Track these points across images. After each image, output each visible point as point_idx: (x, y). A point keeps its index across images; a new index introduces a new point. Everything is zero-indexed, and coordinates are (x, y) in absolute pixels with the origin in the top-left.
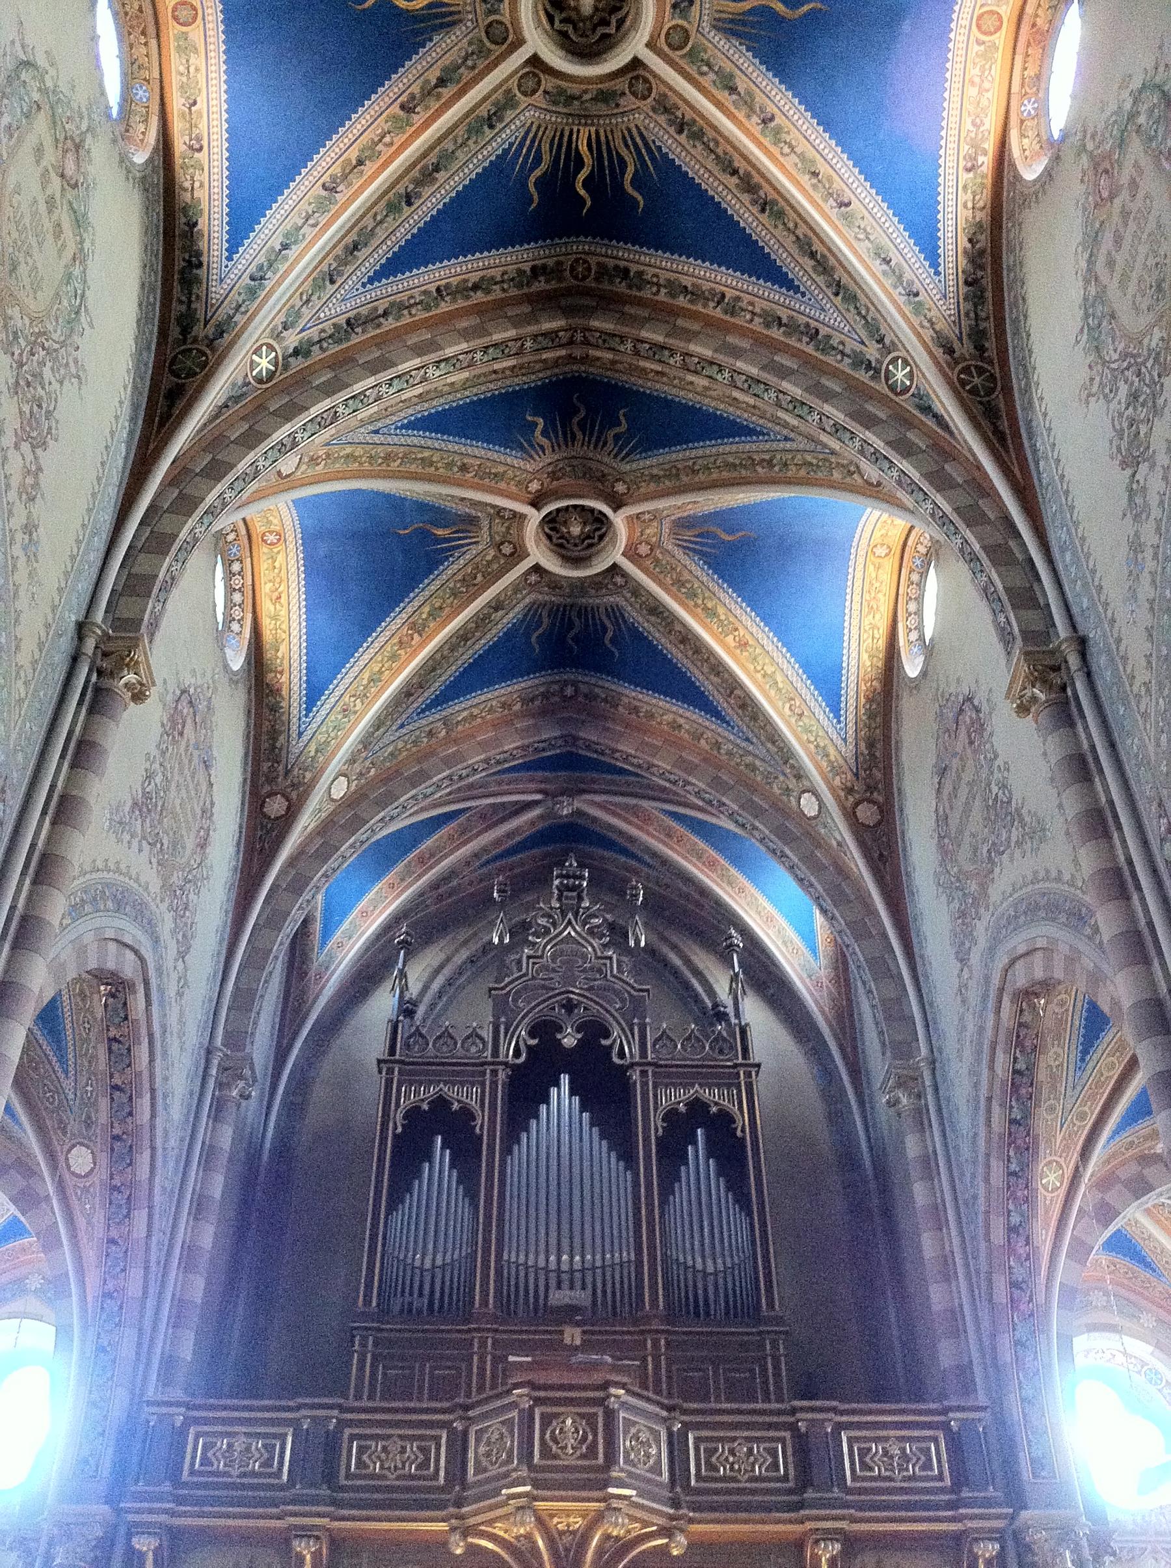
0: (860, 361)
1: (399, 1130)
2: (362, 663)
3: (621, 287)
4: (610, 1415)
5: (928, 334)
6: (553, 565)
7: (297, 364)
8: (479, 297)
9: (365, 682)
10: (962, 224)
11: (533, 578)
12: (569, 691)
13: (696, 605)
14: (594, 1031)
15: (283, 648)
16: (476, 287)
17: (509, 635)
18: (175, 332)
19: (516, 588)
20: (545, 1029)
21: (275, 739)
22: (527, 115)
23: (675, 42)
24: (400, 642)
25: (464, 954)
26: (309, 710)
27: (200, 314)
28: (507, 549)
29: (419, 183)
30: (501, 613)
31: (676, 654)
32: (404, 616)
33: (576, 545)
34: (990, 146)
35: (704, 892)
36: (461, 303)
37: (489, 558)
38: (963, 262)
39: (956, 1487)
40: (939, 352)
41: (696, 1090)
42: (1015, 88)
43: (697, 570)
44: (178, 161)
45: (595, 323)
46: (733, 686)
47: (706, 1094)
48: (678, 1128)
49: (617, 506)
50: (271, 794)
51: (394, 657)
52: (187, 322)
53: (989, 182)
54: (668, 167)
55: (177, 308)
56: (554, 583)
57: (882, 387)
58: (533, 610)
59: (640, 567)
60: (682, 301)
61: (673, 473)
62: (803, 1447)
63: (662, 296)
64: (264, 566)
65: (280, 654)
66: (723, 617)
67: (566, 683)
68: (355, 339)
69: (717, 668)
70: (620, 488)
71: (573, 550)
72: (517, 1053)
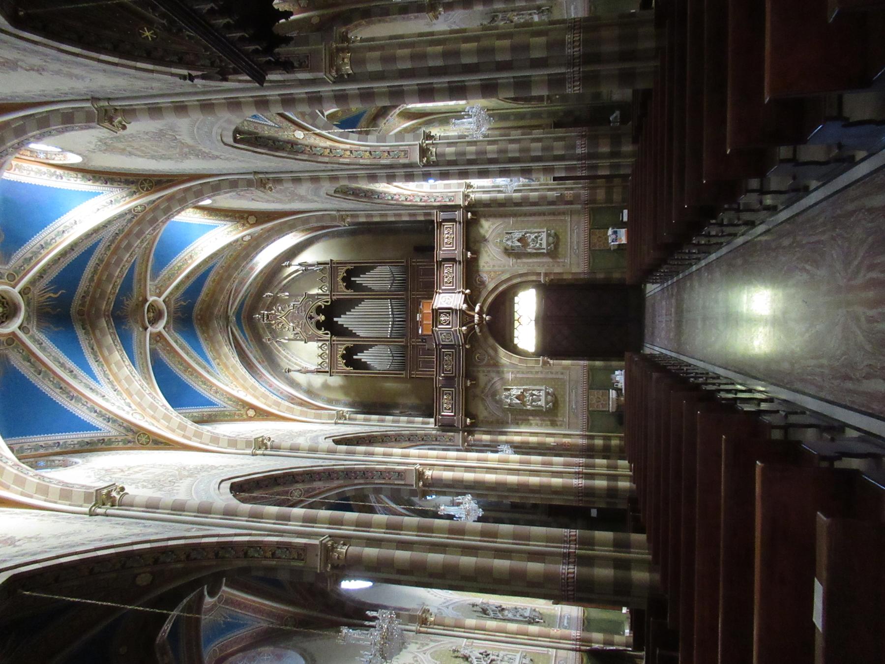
0: (130, 221)
3: (88, 299)
5: (128, 199)
7: (134, 407)
8: (95, 347)
10: (83, 182)
14: (319, 310)
16: (93, 349)
18: (130, 445)
20: (319, 325)
22: (34, 331)
23: (13, 278)
29: (65, 368)
34: (53, 170)
35: (261, 272)
36: (99, 354)
38: (98, 184)
39: (456, 222)
40: (135, 197)
41: (339, 279)
42: (33, 159)
43: (165, 272)
44: (63, 450)
45: (104, 307)
46: (205, 262)
47: (340, 277)
48: (350, 285)
53: (66, 172)
54: (52, 283)
56: (167, 323)
57: (141, 214)
60: (96, 278)
61: (139, 281)
63: (93, 284)
68: (119, 389)
69: (199, 266)
70: (141, 299)
71: (157, 316)
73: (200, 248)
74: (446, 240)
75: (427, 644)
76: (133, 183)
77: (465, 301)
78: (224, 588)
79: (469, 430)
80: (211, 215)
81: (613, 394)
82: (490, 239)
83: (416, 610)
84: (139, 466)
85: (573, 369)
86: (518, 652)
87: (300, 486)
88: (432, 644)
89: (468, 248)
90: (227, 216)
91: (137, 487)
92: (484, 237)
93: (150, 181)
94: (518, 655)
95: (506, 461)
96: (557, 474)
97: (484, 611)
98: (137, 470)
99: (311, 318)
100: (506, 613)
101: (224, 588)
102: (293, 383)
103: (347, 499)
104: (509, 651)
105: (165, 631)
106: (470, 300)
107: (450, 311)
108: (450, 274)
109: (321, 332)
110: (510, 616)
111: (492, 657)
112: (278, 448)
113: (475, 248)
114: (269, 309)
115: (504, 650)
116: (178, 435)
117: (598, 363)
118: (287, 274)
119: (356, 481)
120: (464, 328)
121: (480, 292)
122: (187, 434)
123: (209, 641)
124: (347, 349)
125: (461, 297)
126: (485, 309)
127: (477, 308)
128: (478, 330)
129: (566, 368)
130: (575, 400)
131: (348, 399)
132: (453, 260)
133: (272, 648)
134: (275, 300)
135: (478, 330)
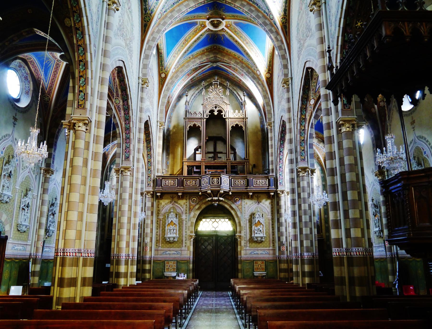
0: (265, 12)
4: (221, 178)
6: (211, 28)
7: (165, 14)
12: (215, 47)
14: (220, 112)
15: (162, 45)
17: (203, 40)
18: (144, 12)
19: (205, 32)
20: (212, 111)
25: (197, 92)
26: (167, 56)
27: (148, 8)
28: (203, 26)
31: (235, 43)
39: (268, 186)
46: (245, 51)
50: (162, 73)
51: (182, 46)
52: (146, 10)
55: (144, 7)
56: (212, 31)
57: (268, 17)
58: (208, 35)
59: (228, 29)
61: (234, 16)
62: (248, 181)
67: (214, 46)
68: (174, 6)
69: (242, 47)
72: (207, 116)
73: (252, 48)
74: (258, 181)
75: (34, 174)
76: (285, 13)
77: (225, 192)
78: (65, 63)
79: (154, 195)
80: (270, 54)
81: (174, 274)
82: (259, 205)
83: (53, 167)
84: (132, 17)
85: (187, 252)
86: (30, 224)
87: (121, 103)
88: (34, 176)
89: (254, 193)
90: (270, 62)
91: (119, 17)
92: (261, 202)
93: (286, 23)
94: (28, 224)
95: (135, 216)
96: (126, 245)
97: (53, 205)
98: (130, 16)
99: (216, 107)
100: (52, 217)
101: (65, 63)
102: (180, 97)
103: (114, 128)
104: (30, 219)
105: (40, 33)
106: (226, 195)
107: (220, 183)
108: (240, 182)
109: (208, 111)
110: (50, 219)
111: (26, 209)
112: (142, 91)
113: (254, 197)
114: (221, 84)
115: (31, 216)
116: (149, 37)
117: (191, 266)
118: (240, 94)
119: (124, 134)
120: (210, 191)
121: (230, 200)
122: (150, 42)
123: (36, 56)
124: (199, 127)
125: (227, 189)
126: (221, 203)
127: (221, 199)
128: (209, 199)
129: (188, 249)
130: (171, 253)
131: (171, 128)
132: (248, 185)
133: (32, 89)
134: (225, 87)
135: (209, 199)
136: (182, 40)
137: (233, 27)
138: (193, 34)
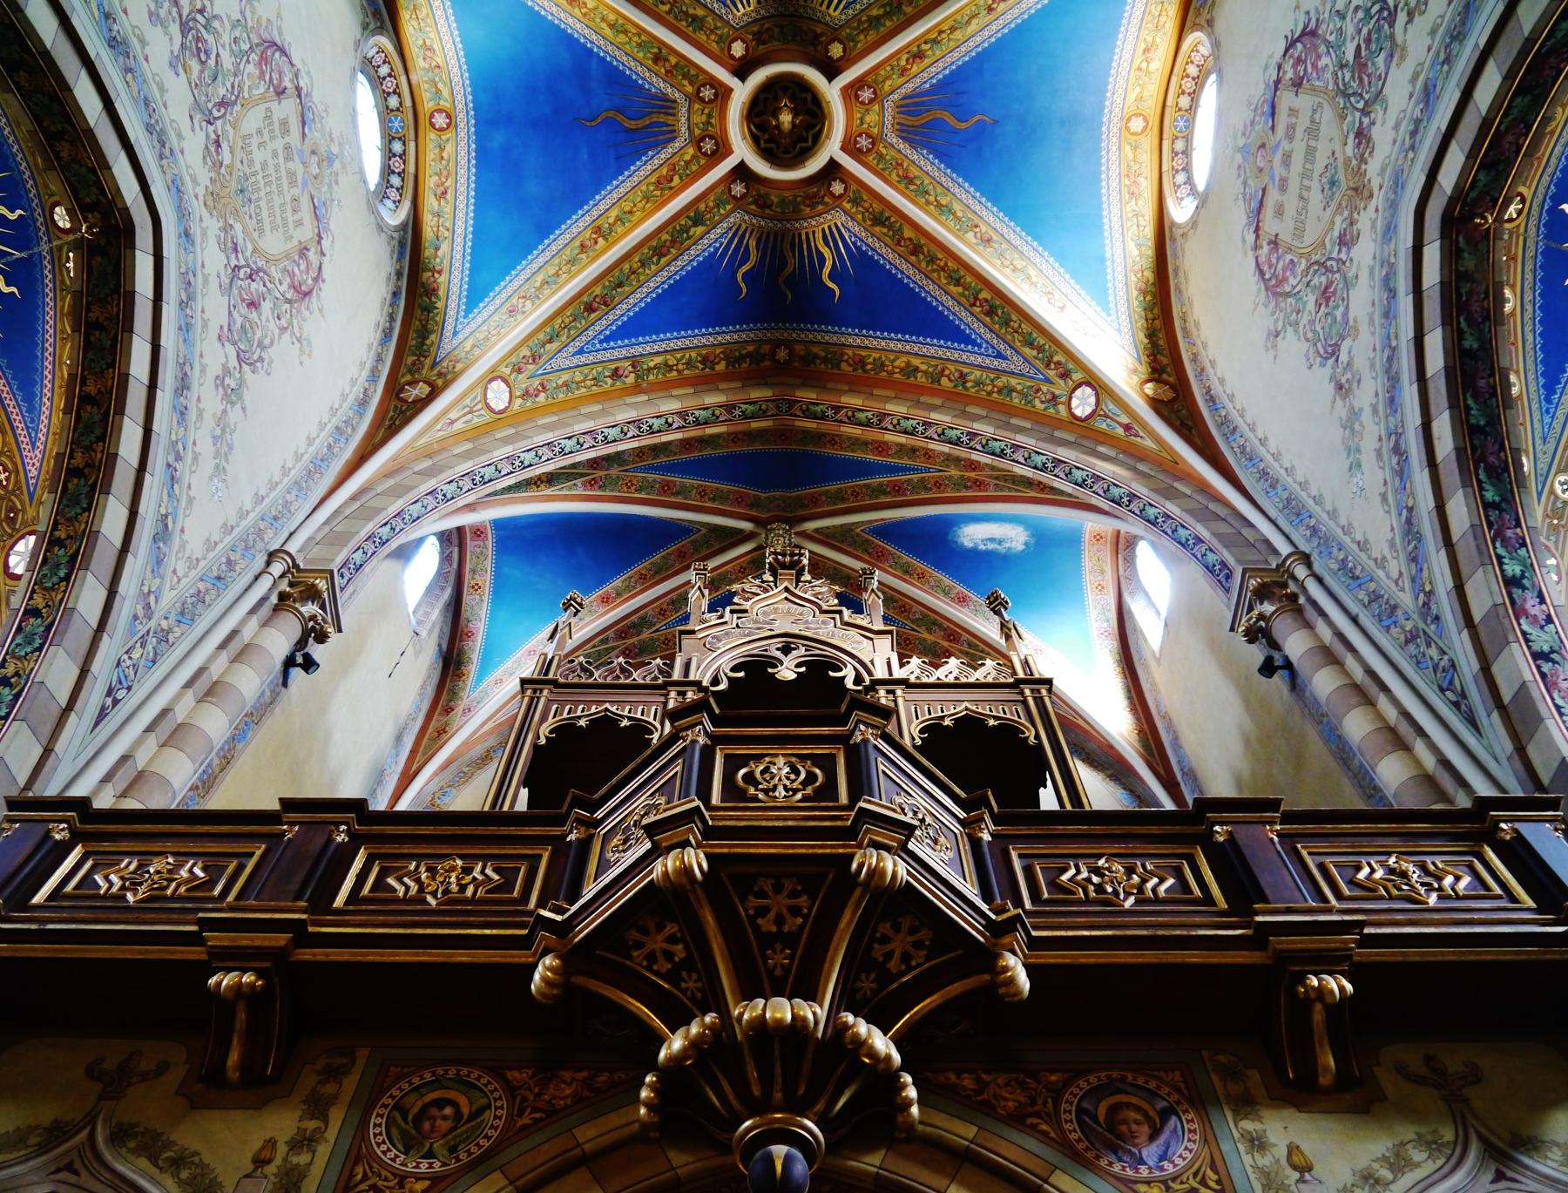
1: (543, 741)
2: (535, 266)
9: (538, 284)
11: (738, 189)
12: (782, 354)
13: (928, 203)
15: (444, 248)
17: (711, 262)
21: (425, 338)
24: (583, 246)
26: (468, 311)
28: (708, 146)
30: (700, 230)
32: (588, 218)
33: (786, 152)
37: (687, 157)
49: (831, 72)
51: (572, 262)
64: (430, 154)
65: (440, 253)
66: (960, 214)
67: (777, 344)
73: (1019, 264)
80: (1144, 293)
90: (1151, 335)
136: (578, 225)
137: (890, 154)
138: (647, 198)
